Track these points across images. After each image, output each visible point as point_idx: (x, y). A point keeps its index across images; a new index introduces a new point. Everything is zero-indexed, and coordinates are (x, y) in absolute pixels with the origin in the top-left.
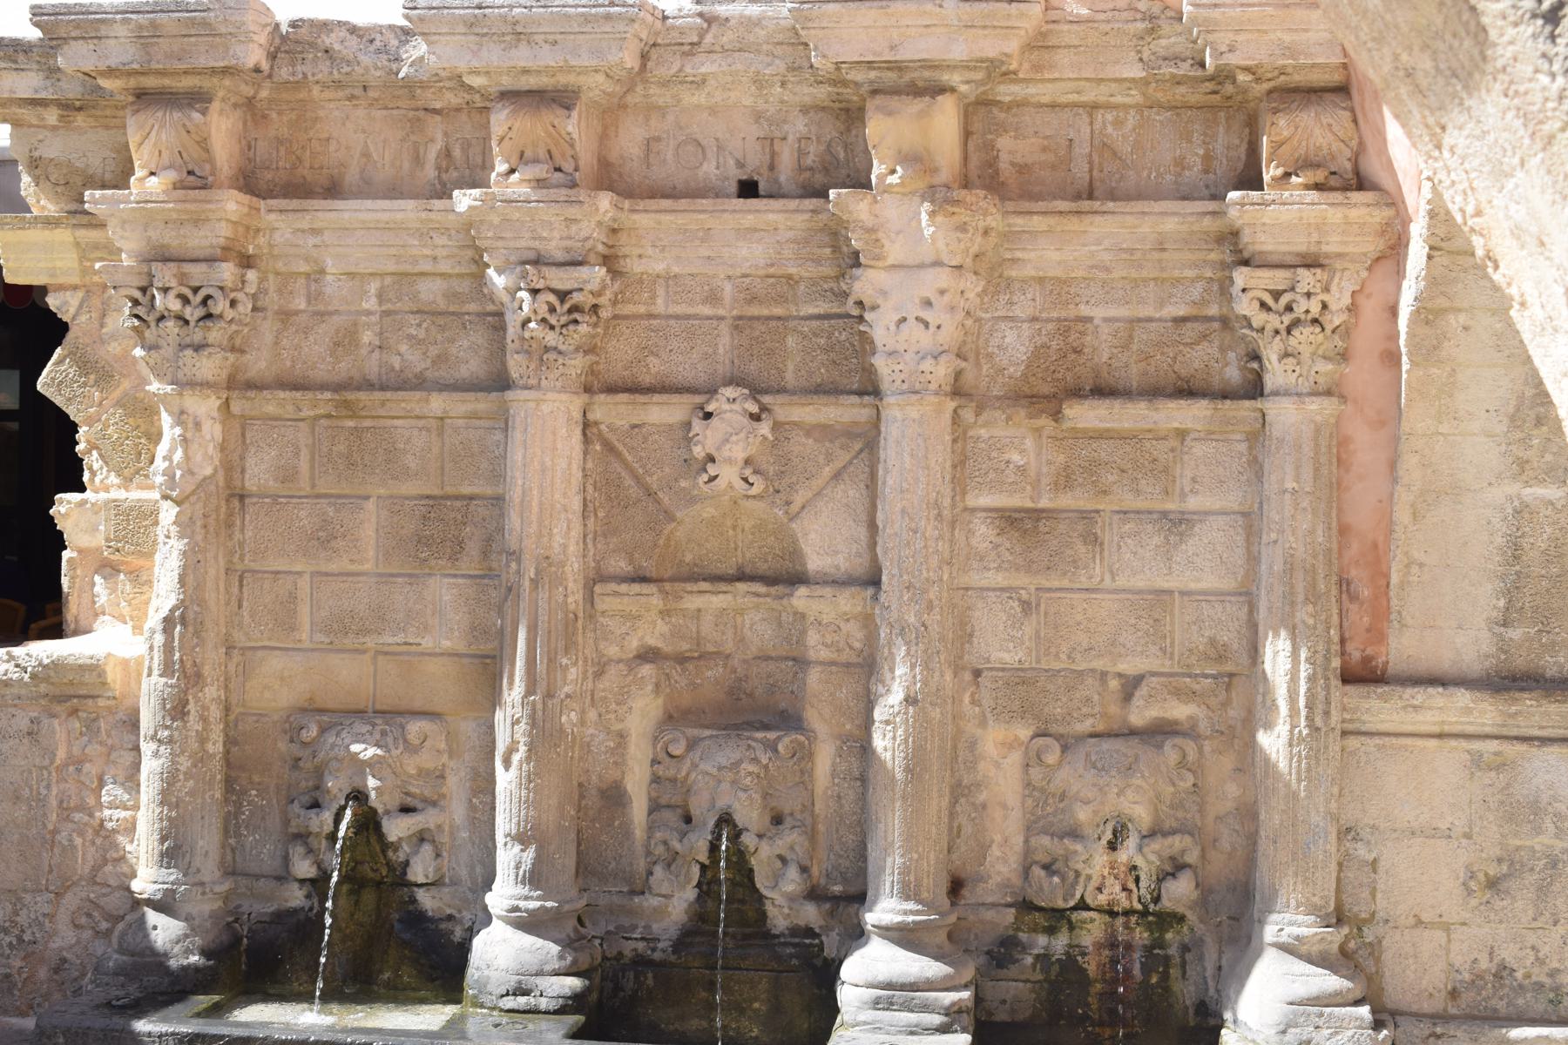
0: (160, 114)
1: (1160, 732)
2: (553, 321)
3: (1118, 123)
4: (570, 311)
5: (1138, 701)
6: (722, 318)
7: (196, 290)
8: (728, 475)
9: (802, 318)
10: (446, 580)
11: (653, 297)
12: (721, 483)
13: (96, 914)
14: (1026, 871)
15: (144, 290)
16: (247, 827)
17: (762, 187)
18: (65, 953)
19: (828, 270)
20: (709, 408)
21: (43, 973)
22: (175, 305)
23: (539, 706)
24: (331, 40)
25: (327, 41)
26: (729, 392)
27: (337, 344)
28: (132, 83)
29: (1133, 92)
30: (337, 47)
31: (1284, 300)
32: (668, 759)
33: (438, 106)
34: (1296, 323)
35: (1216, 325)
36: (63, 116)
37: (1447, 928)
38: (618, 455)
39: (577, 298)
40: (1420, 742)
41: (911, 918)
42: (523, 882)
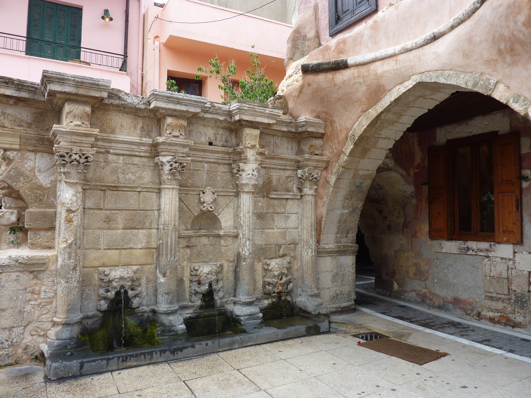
0: (76, 106)
2: (178, 170)
3: (277, 139)
4: (182, 168)
7: (83, 155)
10: (140, 231)
11: (190, 166)
13: (39, 330)
14: (264, 287)
15: (67, 153)
16: (85, 300)
17: (214, 143)
18: (28, 344)
20: (204, 191)
21: (20, 351)
22: (78, 158)
23: (173, 261)
24: (121, 95)
25: (120, 95)
26: (209, 188)
27: (112, 172)
28: (68, 97)
30: (122, 97)
32: (194, 271)
33: (141, 115)
36: (16, 102)
38: (183, 201)
39: (185, 164)
41: (251, 300)
42: (169, 304)
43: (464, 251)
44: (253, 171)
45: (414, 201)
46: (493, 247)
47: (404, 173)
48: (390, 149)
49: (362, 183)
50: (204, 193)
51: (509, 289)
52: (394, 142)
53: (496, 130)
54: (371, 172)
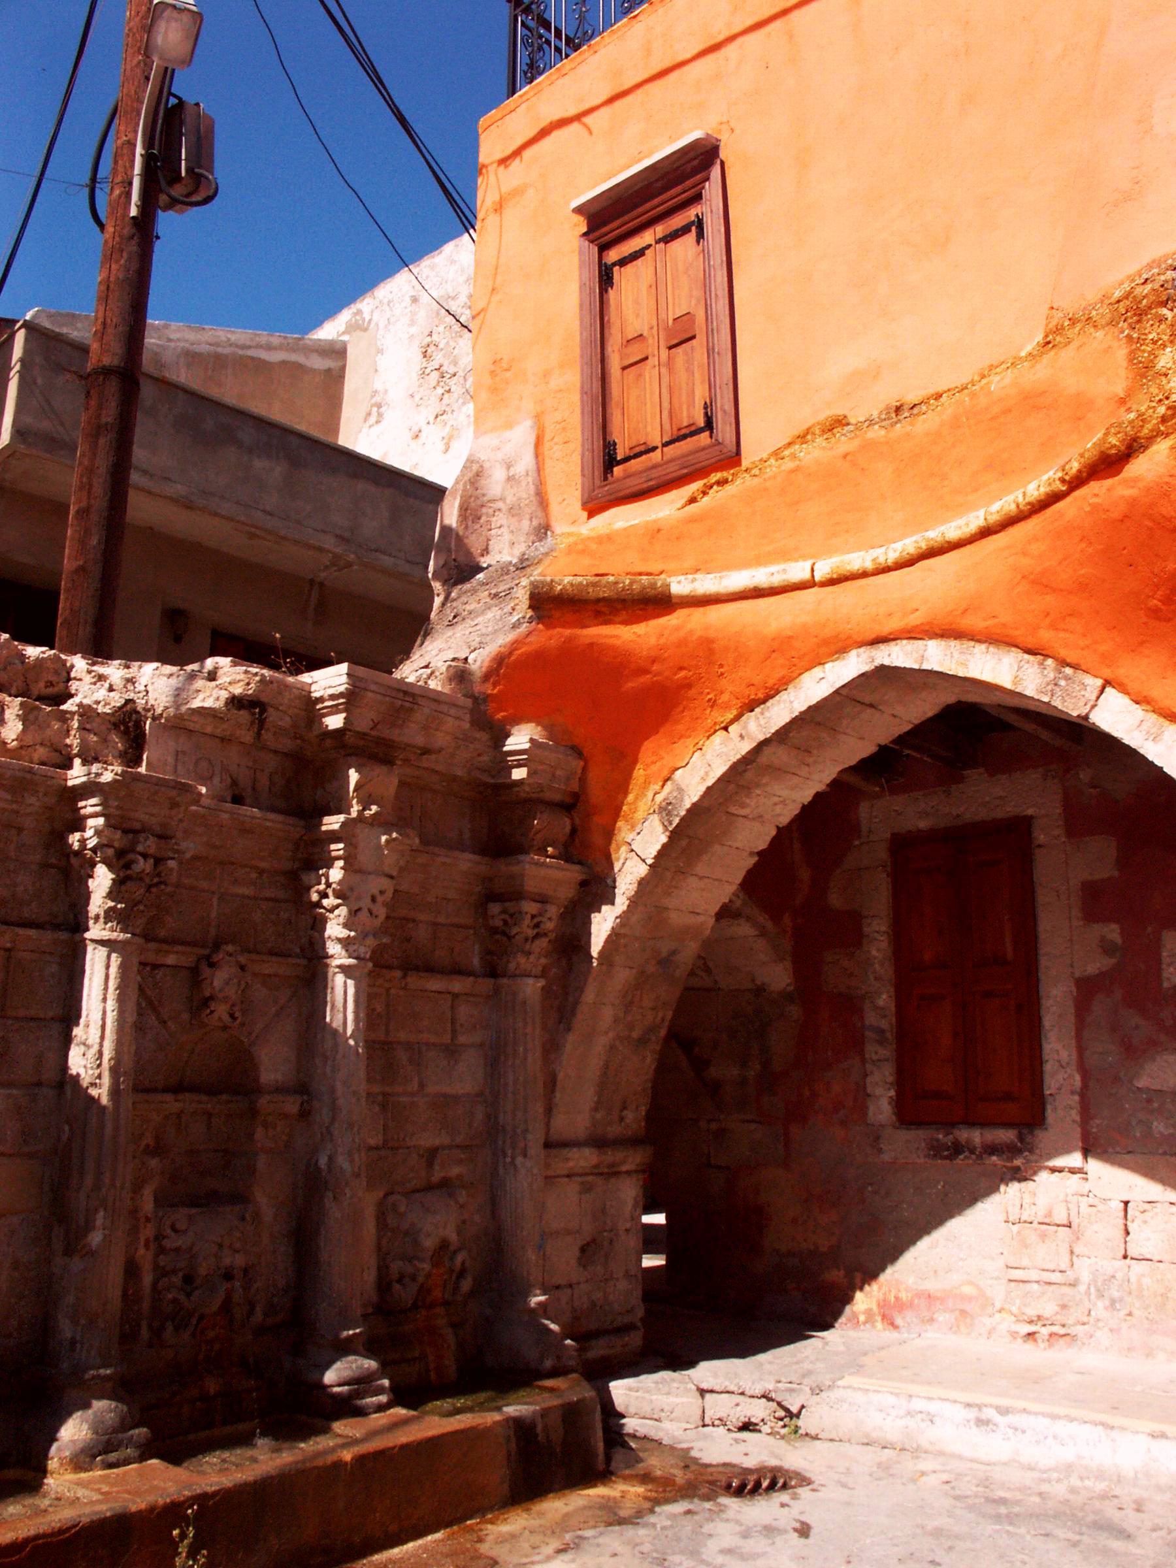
1: (445, 1184)
5: (437, 1168)
6: (213, 893)
8: (221, 1010)
9: (261, 899)
12: (216, 1015)
17: (248, 801)
19: (288, 866)
26: (230, 948)
29: (444, 784)
31: (535, 921)
32: (173, 1234)
34: (537, 936)
35: (472, 932)
37: (570, 1286)
40: (559, 1180)
43: (946, 1153)
44: (373, 899)
45: (795, 1011)
46: (1028, 1139)
47: (769, 925)
48: (760, 854)
49: (674, 953)
50: (212, 965)
51: (1072, 1252)
52: (774, 832)
53: (1030, 812)
54: (701, 919)
